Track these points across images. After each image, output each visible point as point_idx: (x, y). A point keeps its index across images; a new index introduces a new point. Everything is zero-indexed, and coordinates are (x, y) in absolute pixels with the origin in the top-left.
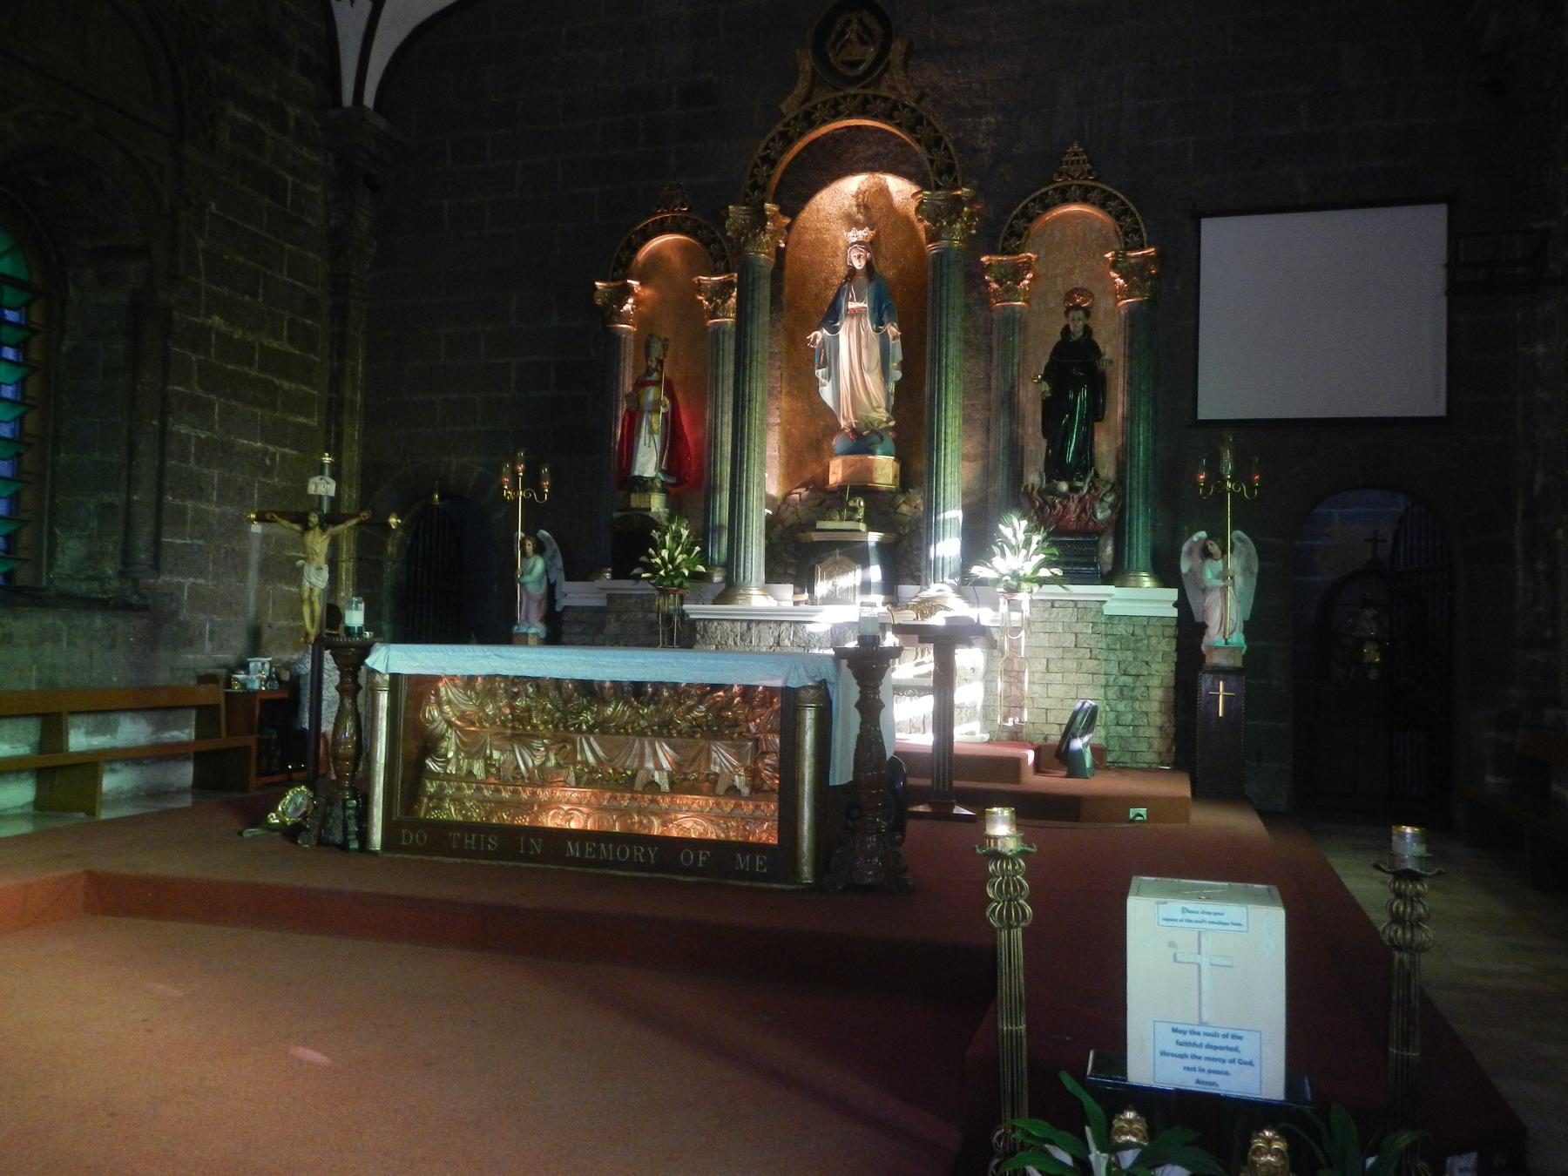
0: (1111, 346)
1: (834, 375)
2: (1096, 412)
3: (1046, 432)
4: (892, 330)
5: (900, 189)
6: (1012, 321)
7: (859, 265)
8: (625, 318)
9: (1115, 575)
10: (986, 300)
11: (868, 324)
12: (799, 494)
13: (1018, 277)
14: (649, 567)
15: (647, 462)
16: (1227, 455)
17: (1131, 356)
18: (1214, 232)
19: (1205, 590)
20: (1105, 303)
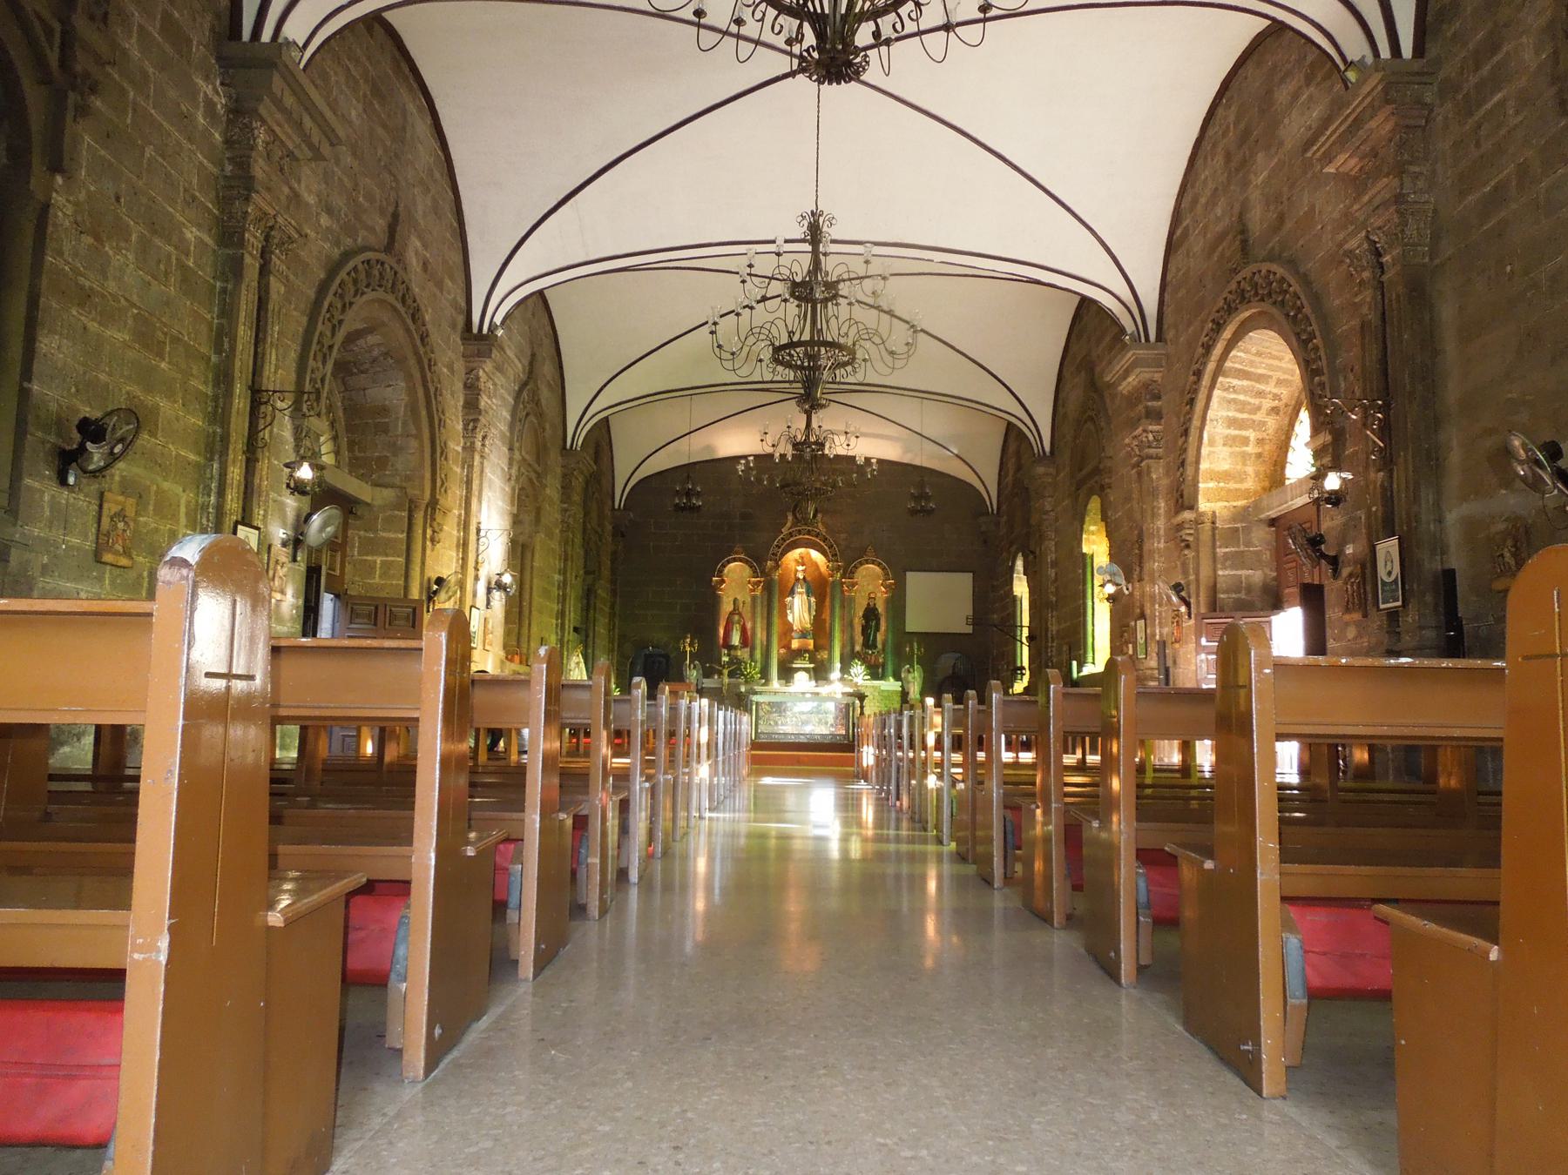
0: (880, 610)
1: (792, 612)
2: (877, 629)
3: (863, 634)
4: (813, 599)
5: (816, 556)
6: (852, 599)
7: (801, 577)
8: (721, 590)
9: (883, 677)
10: (843, 592)
11: (805, 597)
12: (782, 651)
13: (853, 585)
14: (743, 675)
15: (736, 639)
16: (915, 644)
17: (887, 612)
18: (909, 575)
19: (908, 682)
20: (879, 595)
